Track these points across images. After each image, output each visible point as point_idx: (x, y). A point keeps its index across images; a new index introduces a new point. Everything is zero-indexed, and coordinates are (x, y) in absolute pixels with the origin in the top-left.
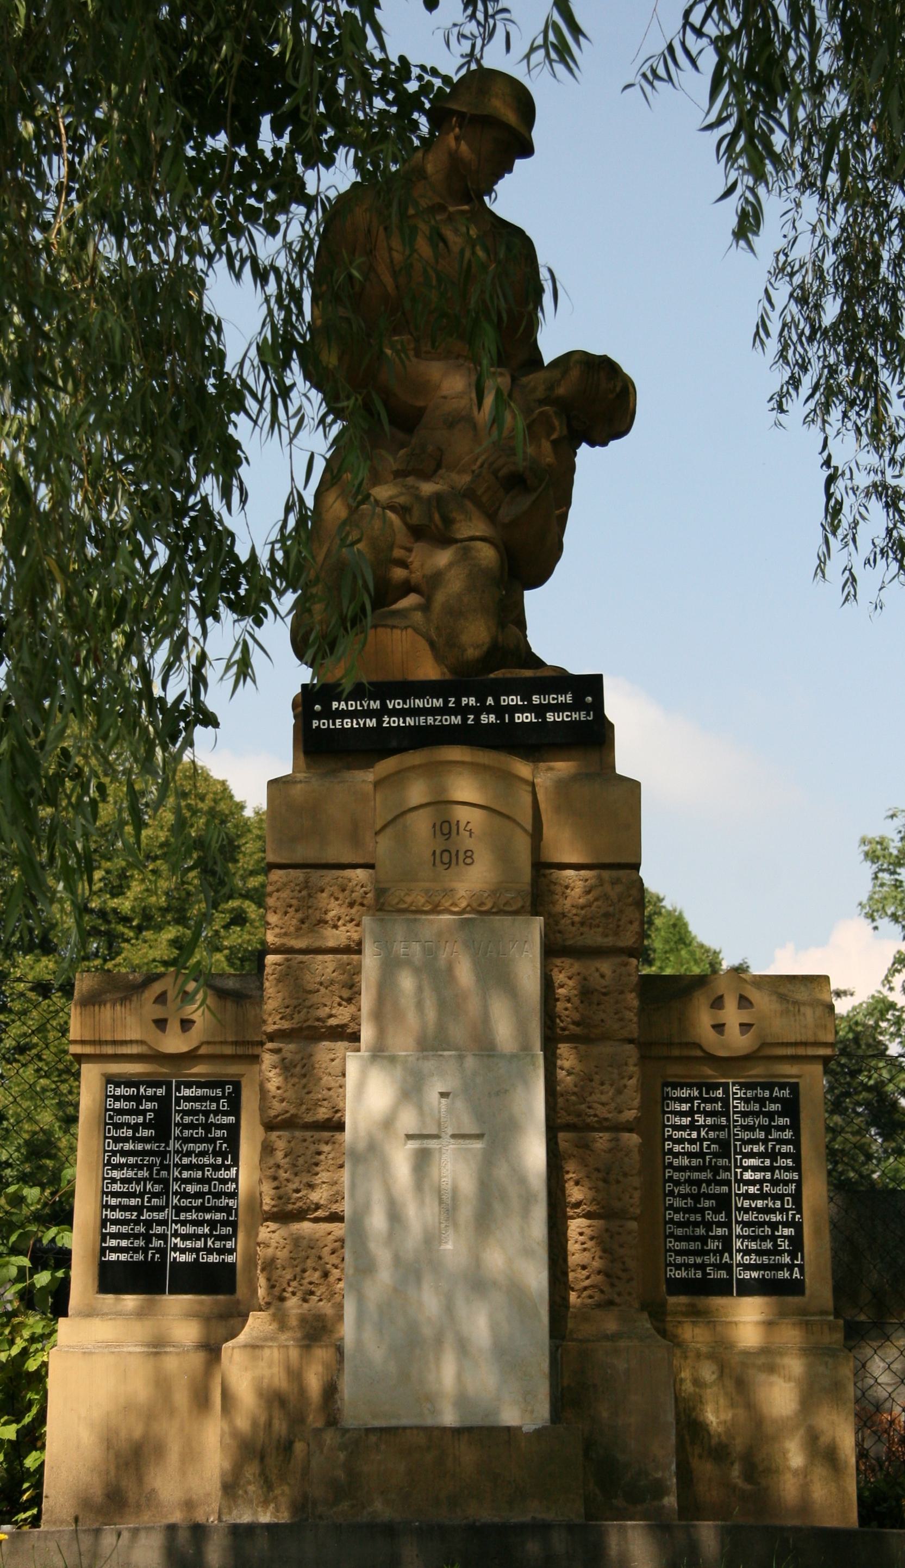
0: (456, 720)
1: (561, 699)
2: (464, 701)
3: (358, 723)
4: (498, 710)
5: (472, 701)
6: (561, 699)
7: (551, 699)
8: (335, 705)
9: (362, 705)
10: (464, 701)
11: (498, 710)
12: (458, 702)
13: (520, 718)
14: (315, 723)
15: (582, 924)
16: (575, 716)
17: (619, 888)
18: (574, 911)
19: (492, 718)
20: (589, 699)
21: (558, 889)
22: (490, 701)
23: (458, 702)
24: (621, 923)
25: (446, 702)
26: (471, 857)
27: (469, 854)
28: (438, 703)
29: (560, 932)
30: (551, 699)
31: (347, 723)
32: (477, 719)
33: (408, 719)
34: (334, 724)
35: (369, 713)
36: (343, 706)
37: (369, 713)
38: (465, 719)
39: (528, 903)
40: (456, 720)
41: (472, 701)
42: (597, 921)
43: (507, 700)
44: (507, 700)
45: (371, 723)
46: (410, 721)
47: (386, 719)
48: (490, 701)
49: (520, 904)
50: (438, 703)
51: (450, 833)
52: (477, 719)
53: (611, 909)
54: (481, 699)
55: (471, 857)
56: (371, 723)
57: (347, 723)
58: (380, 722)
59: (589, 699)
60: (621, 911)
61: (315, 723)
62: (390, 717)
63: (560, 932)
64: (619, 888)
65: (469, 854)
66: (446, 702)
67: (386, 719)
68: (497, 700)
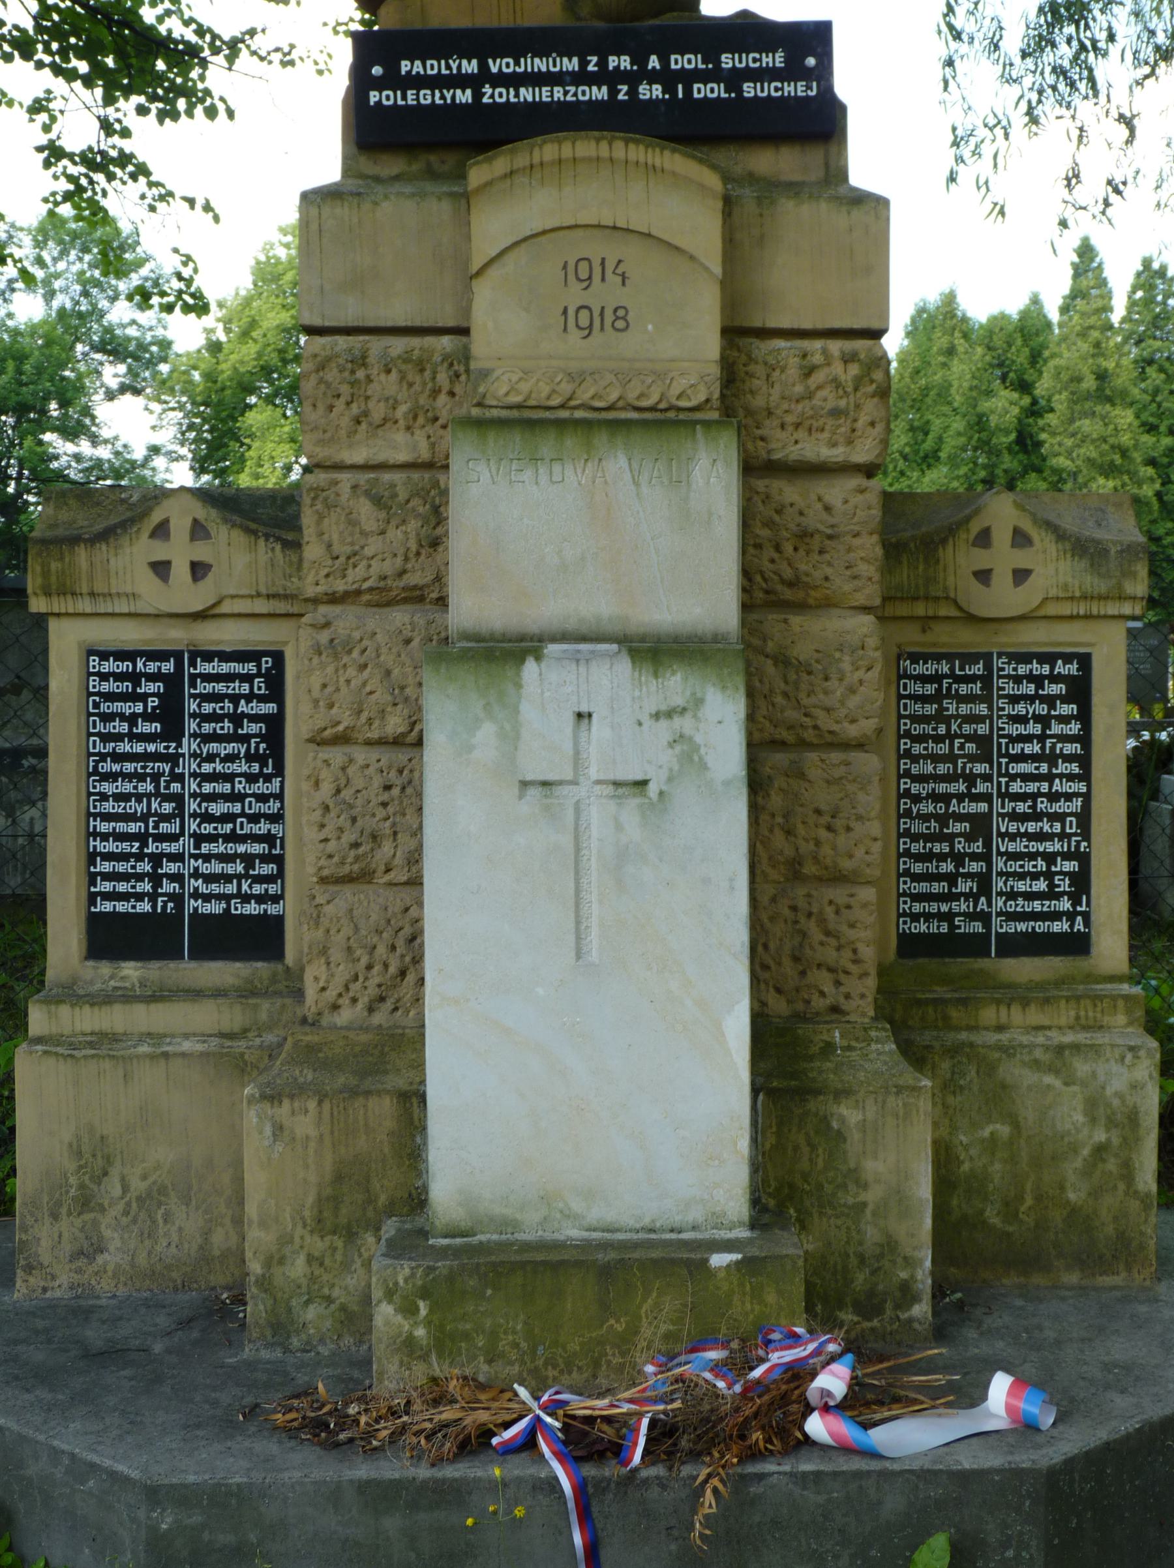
0: (600, 93)
1: (767, 60)
2: (613, 62)
3: (443, 97)
4: (667, 78)
5: (625, 62)
6: (767, 60)
7: (748, 60)
8: (405, 66)
9: (448, 67)
10: (613, 62)
11: (667, 78)
12: (602, 63)
13: (700, 91)
14: (374, 96)
15: (797, 426)
16: (789, 89)
17: (854, 370)
18: (785, 406)
19: (657, 91)
20: (811, 61)
21: (759, 370)
22: (654, 62)
23: (602, 63)
24: (860, 424)
25: (584, 63)
26: (624, 318)
27: (621, 313)
28: (571, 64)
29: (762, 439)
30: (748, 60)
31: (426, 97)
32: (633, 92)
33: (522, 90)
34: (404, 98)
35: (461, 81)
36: (418, 67)
37: (461, 81)
38: (613, 92)
39: (716, 395)
40: (600, 93)
41: (625, 62)
42: (821, 423)
43: (678, 62)
44: (678, 62)
45: (465, 96)
46: (526, 94)
47: (487, 89)
48: (654, 62)
49: (702, 397)
50: (571, 64)
51: (590, 278)
52: (633, 92)
53: (842, 403)
54: (640, 59)
55: (624, 318)
56: (465, 96)
57: (426, 97)
58: (478, 95)
59: (811, 61)
60: (858, 406)
61: (374, 96)
62: (494, 87)
63: (762, 439)
64: (854, 370)
65: (621, 313)
66: (584, 63)
67: (487, 89)
68: (665, 61)
